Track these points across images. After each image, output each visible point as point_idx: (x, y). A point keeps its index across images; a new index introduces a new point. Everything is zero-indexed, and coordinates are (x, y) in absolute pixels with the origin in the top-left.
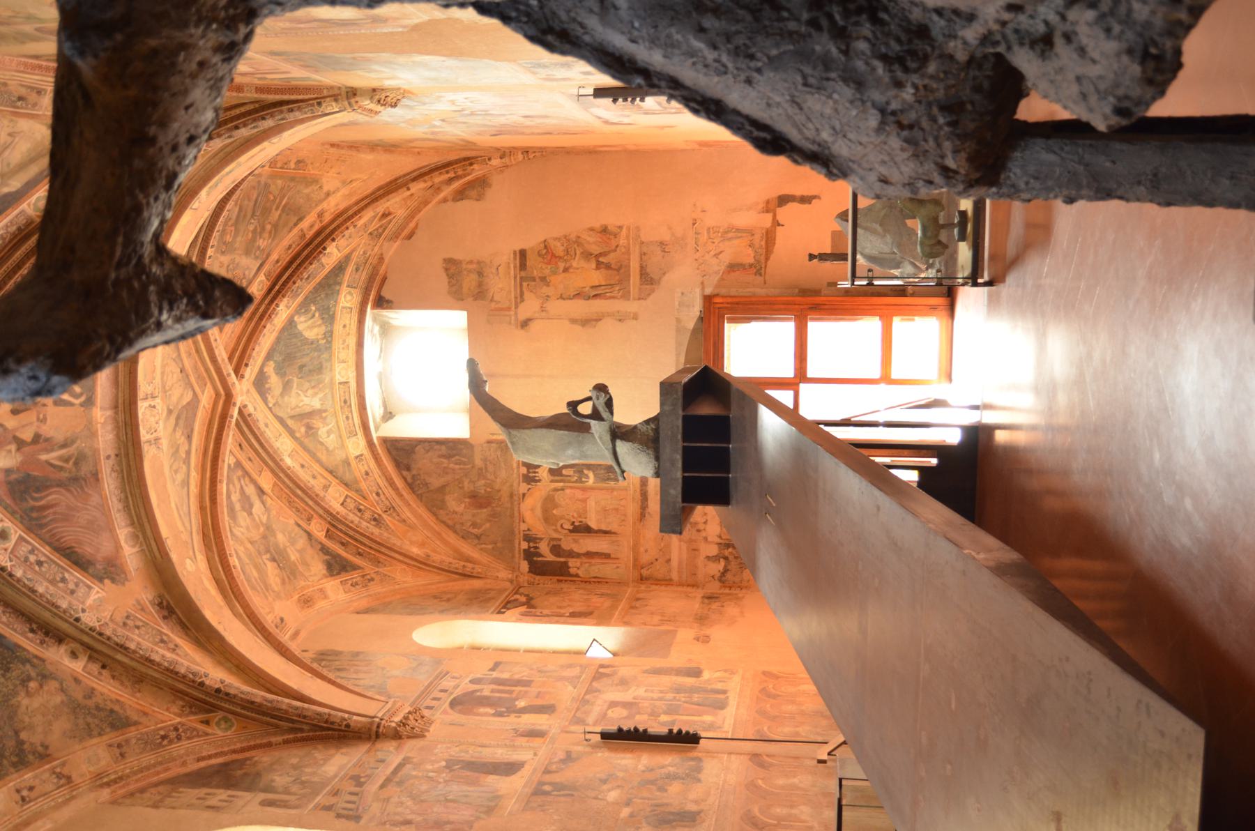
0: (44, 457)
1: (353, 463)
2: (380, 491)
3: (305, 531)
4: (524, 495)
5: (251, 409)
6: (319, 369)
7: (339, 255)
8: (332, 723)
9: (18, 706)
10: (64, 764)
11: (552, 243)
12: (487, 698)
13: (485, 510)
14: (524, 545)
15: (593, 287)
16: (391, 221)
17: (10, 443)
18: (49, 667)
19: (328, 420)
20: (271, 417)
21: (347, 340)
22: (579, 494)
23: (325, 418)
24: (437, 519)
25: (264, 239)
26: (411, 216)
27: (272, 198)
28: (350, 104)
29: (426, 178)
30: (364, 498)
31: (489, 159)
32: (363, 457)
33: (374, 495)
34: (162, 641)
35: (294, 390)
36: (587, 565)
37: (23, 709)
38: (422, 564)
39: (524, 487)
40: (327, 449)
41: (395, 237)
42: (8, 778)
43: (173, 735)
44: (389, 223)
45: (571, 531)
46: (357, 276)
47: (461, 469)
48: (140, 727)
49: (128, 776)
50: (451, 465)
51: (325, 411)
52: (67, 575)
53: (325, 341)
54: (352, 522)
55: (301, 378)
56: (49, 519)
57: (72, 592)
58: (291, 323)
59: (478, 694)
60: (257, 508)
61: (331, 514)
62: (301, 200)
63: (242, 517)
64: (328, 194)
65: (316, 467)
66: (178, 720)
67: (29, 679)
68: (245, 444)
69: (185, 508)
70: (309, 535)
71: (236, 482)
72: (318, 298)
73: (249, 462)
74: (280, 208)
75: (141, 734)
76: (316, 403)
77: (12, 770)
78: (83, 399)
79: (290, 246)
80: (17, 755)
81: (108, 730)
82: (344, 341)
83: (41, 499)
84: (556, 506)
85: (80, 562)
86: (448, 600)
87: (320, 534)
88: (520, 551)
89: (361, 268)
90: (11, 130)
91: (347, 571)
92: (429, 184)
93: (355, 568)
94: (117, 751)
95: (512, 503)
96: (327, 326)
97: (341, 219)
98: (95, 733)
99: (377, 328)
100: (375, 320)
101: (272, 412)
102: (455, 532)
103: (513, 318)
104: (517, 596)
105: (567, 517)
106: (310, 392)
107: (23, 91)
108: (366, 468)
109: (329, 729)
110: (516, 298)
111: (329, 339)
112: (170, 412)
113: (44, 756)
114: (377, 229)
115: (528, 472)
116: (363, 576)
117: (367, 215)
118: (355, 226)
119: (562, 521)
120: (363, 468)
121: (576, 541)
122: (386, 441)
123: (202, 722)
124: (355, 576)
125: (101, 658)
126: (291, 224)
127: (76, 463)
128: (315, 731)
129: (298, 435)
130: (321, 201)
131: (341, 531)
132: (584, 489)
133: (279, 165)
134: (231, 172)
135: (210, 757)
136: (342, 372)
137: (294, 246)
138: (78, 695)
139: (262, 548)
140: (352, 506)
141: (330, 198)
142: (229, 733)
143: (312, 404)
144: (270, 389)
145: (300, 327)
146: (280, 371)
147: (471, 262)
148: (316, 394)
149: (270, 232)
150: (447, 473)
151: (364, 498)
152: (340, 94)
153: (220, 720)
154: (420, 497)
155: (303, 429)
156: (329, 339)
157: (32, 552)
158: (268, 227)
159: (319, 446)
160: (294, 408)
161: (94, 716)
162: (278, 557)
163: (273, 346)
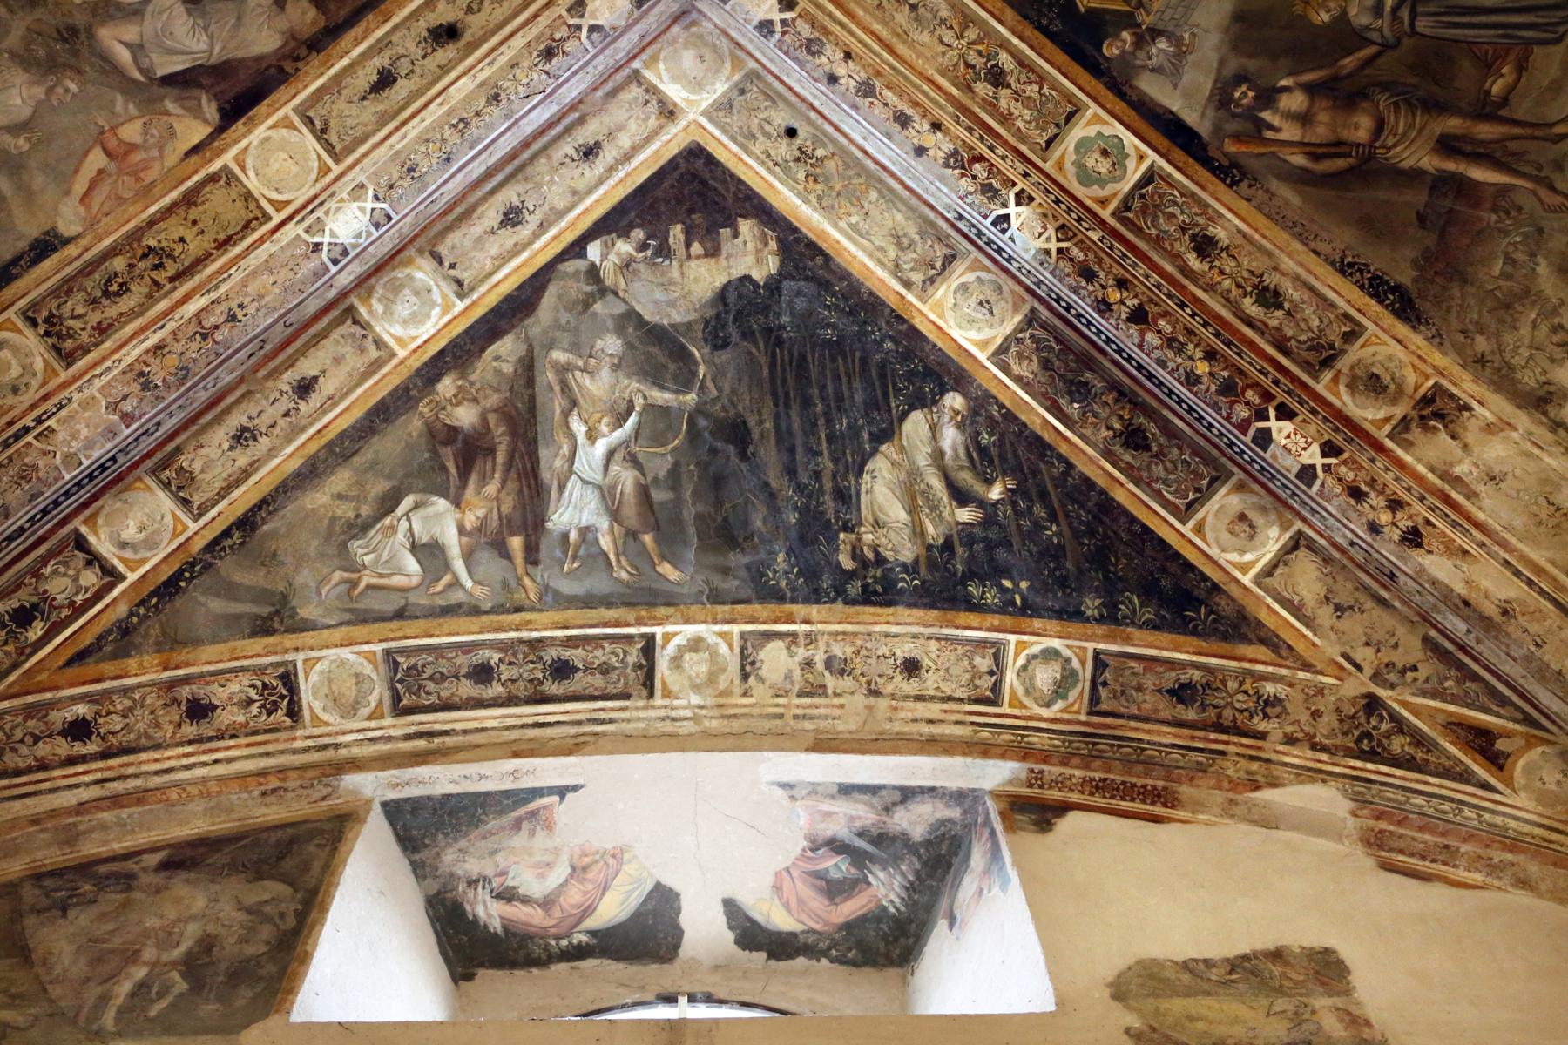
1: (261, 653)
2: (91, 748)
7: (1247, 580)
16: (1465, 777)
20: (544, 248)
21: (847, 683)
25: (1304, 119)
27: (1497, 88)
30: (81, 656)
32: (280, 716)
33: (82, 709)
40: (361, 527)
44: (1446, 773)
46: (1149, 701)
47: (105, 999)
51: (532, 555)
53: (846, 562)
55: (694, 434)
65: (285, 459)
72: (1039, 511)
73: (368, 75)
74: (1451, 166)
79: (1270, 297)
82: (839, 668)
89: (1191, 715)
96: (911, 569)
101: (562, 257)
106: (627, 478)
108: (225, 717)
111: (854, 588)
114: (1400, 726)
126: (1379, 260)
129: (447, 386)
130: (1503, 380)
137: (1276, 318)
140: (58, 587)
141: (1523, 420)
143: (573, 485)
144: (664, 251)
145: (916, 425)
148: (615, 515)
149: (1337, 147)
150: (97, 960)
151: (81, 656)
155: (465, 417)
156: (854, 588)
158: (1360, 128)
159: (379, 487)
160: (565, 387)
163: (845, 276)
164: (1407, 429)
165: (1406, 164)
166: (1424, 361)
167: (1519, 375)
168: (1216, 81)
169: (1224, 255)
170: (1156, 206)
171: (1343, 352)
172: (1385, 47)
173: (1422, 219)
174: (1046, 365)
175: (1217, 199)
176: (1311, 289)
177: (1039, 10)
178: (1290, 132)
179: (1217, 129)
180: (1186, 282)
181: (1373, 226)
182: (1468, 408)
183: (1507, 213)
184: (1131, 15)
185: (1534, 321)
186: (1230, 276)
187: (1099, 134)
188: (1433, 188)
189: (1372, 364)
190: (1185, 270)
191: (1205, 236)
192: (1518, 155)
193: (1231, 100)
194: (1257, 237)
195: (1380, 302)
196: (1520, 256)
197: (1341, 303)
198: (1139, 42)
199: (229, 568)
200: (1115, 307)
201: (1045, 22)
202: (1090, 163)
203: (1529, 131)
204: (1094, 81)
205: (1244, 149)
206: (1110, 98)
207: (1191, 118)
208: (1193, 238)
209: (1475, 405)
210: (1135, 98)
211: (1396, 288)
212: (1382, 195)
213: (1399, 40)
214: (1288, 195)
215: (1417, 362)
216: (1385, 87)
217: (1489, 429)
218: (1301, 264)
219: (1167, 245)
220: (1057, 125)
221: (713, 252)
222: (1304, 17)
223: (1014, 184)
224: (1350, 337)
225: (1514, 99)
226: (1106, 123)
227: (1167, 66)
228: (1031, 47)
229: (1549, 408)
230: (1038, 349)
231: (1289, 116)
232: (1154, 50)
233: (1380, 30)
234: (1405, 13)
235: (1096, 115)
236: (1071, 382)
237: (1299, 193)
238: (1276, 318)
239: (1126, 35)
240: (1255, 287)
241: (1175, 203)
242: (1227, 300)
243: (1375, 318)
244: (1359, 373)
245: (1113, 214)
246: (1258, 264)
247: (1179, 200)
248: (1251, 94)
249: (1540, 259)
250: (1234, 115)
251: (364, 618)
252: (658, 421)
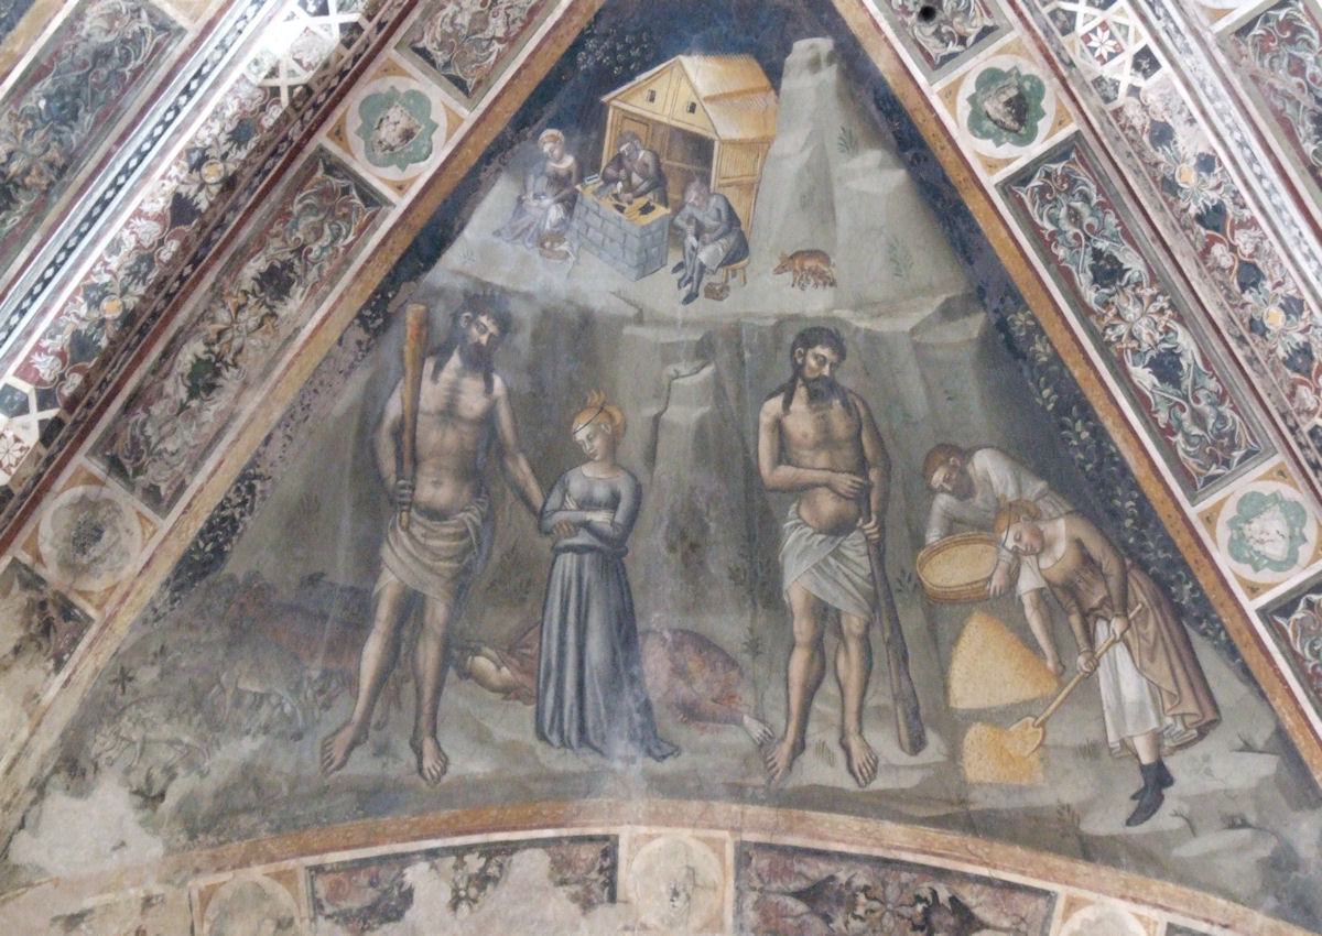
25: (449, 412)
27: (483, 663)
62: (251, 686)
74: (384, 611)
79: (204, 380)
126: (258, 526)
130: (101, 710)
137: (175, 389)
141: (47, 741)
149: (410, 458)
158: (435, 489)
164: (26, 585)
165: (386, 552)
166: (122, 602)
167: (106, 730)
168: (503, 290)
169: (264, 310)
170: (331, 211)
171: (131, 487)
172: (540, 515)
173: (313, 580)
174: (102, 55)
175: (341, 297)
176: (219, 435)
177: (607, 35)
178: (431, 395)
179: (439, 293)
180: (225, 258)
181: (303, 517)
182: (59, 664)
183: (321, 692)
184: (595, 168)
185: (180, 742)
186: (235, 320)
187: (434, 127)
188: (355, 591)
189: (115, 530)
190: (243, 256)
191: (290, 282)
192: (396, 699)
193: (477, 312)
194: (289, 356)
195: (201, 534)
196: (265, 712)
197: (199, 479)
198: (559, 181)
200: (195, 175)
201: (591, 44)
202: (394, 114)
203: (427, 709)
204: (508, 116)
205: (410, 331)
206: (485, 140)
207: (453, 257)
208: (288, 266)
209: (63, 675)
210: (483, 176)
211: (220, 553)
212: (346, 523)
213: (548, 533)
214: (350, 392)
215: (120, 592)
216: (489, 518)
217: (32, 697)
218: (251, 420)
219: (277, 228)
220: (447, 65)
222: (584, 406)
223: (370, 18)
224: (152, 495)
225: (469, 685)
226: (449, 135)
227: (526, 220)
228: (557, 26)
229: (63, 775)
230: (124, 42)
231: (454, 391)
232: (547, 202)
233: (562, 507)
234: (583, 539)
235: (461, 120)
236: (77, 95)
237: (349, 412)
238: (175, 389)
239: (569, 161)
240: (220, 358)
241: (336, 238)
242: (201, 318)
243: (179, 528)
244: (102, 513)
245: (321, 149)
246: (252, 361)
247: (341, 243)
248: (484, 339)
249: (262, 739)
250: (455, 317)
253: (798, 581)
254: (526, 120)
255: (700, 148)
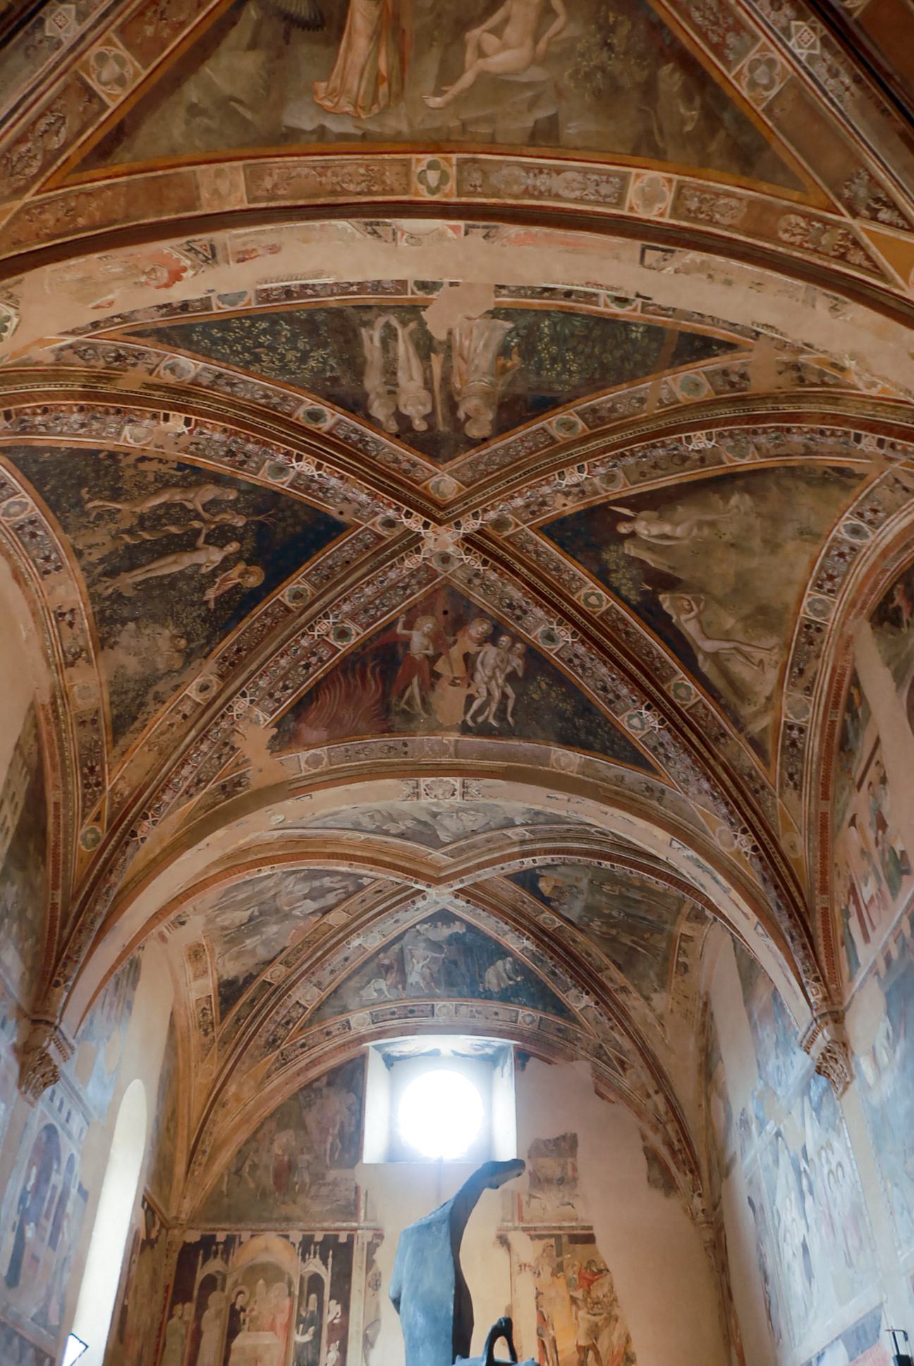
0: (415, 681)
1: (342, 1018)
3: (275, 958)
4: (287, 1237)
5: (420, 904)
6: (451, 984)
8: (65, 965)
9: (163, 626)
10: (89, 661)
11: (605, 1280)
12: (48, 1180)
13: (271, 1182)
14: (221, 1237)
15: (554, 1341)
17: (435, 649)
18: (198, 661)
19: (394, 991)
22: (282, 1319)
23: (396, 987)
24: (266, 1118)
26: (622, 1095)
28: (824, 1015)
29: (671, 1114)
31: (700, 1195)
34: (200, 781)
35: (431, 954)
36: (184, 1331)
37: (159, 630)
38: (215, 1100)
39: (297, 1237)
40: (362, 988)
41: (598, 1076)
42: (89, 602)
43: (92, 780)
45: (233, 1305)
48: (110, 746)
49: (57, 725)
50: (330, 1139)
51: (404, 988)
52: (290, 691)
54: (277, 1013)
56: (351, 680)
57: (271, 695)
58: (503, 953)
59: (55, 1167)
60: (311, 905)
61: (289, 989)
63: (304, 888)
64: (647, 999)
65: (344, 975)
66: (108, 788)
67: (189, 641)
68: (381, 896)
69: (332, 824)
70: (269, 962)
71: (344, 884)
75: (102, 746)
76: (413, 978)
77: (97, 608)
78: (470, 723)
79: (589, 955)
80: (111, 616)
81: (115, 712)
82: (479, 1013)
83: (373, 674)
84: (269, 1284)
85: (299, 709)
86: (168, 1130)
87: (266, 976)
88: (214, 1230)
90: (766, 661)
91: (221, 1004)
92: (664, 1118)
93: (223, 1014)
94: (88, 718)
95: (277, 1220)
97: (619, 1014)
98: (115, 698)
99: (489, 1051)
100: (501, 1050)
102: (248, 1142)
103: (510, 1224)
104: (157, 1227)
105: (252, 1303)
106: (427, 971)
107: (809, 674)
109: (58, 960)
110: (535, 1229)
112: (434, 815)
113: (103, 643)
114: (606, 1054)
115: (316, 1244)
116: (212, 1023)
117: (627, 1044)
118: (612, 1028)
119: (247, 1294)
120: (334, 1029)
121: (218, 1314)
122: (364, 1057)
123: (99, 813)
124: (214, 1014)
125: (196, 715)
127: (404, 711)
128: (59, 944)
129: (381, 956)
130: (640, 991)
131: (268, 999)
132: (288, 1328)
133: (683, 944)
134: (717, 882)
135: (57, 817)
136: (444, 1006)
138: (161, 687)
139: (265, 907)
140: (294, 1014)
142: (80, 842)
145: (500, 963)
146: (455, 939)
147: (575, 1169)
151: (302, 1029)
152: (833, 1004)
153: (97, 833)
154: (295, 1097)
155: (386, 962)
157: (320, 660)
158: (614, 932)
161: (134, 699)
162: (253, 925)
199: (332, 1002)
221: (449, 927)
243: (612, 967)
251: (364, 1007)
252: (434, 960)
253: (639, 898)
254: (549, 906)
255: (555, 887)
